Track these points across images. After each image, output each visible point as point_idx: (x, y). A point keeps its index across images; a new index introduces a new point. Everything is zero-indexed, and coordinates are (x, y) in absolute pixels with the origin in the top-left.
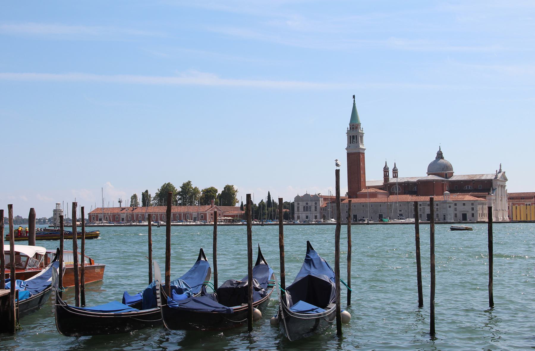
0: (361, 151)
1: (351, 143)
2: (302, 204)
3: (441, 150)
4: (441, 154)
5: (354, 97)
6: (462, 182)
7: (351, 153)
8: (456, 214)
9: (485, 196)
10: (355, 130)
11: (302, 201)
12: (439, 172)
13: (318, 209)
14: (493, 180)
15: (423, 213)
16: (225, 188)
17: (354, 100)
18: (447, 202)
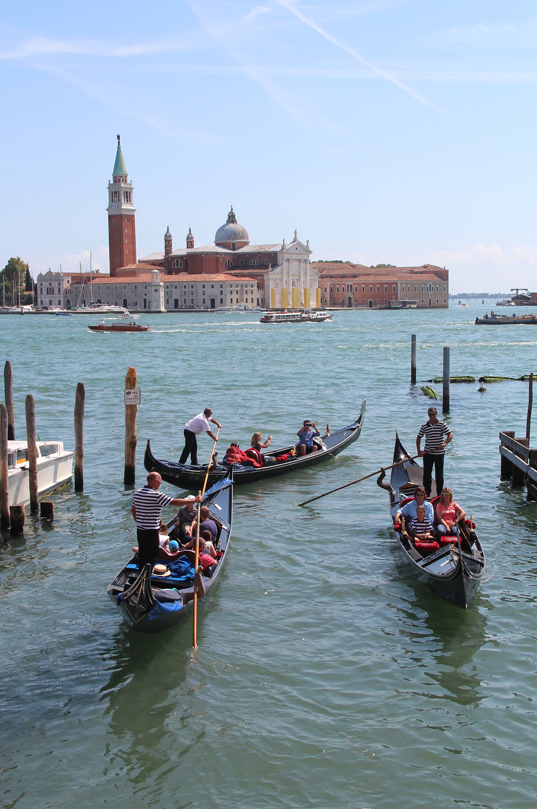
0: (124, 213)
1: (113, 202)
2: (46, 285)
3: (233, 211)
4: (232, 216)
5: (118, 137)
6: (248, 254)
7: (113, 215)
8: (204, 300)
9: (263, 275)
10: (117, 184)
11: (46, 280)
12: (225, 241)
13: (62, 291)
14: (278, 252)
15: (171, 297)
16: (9, 262)
17: (119, 142)
18: (152, 284)
